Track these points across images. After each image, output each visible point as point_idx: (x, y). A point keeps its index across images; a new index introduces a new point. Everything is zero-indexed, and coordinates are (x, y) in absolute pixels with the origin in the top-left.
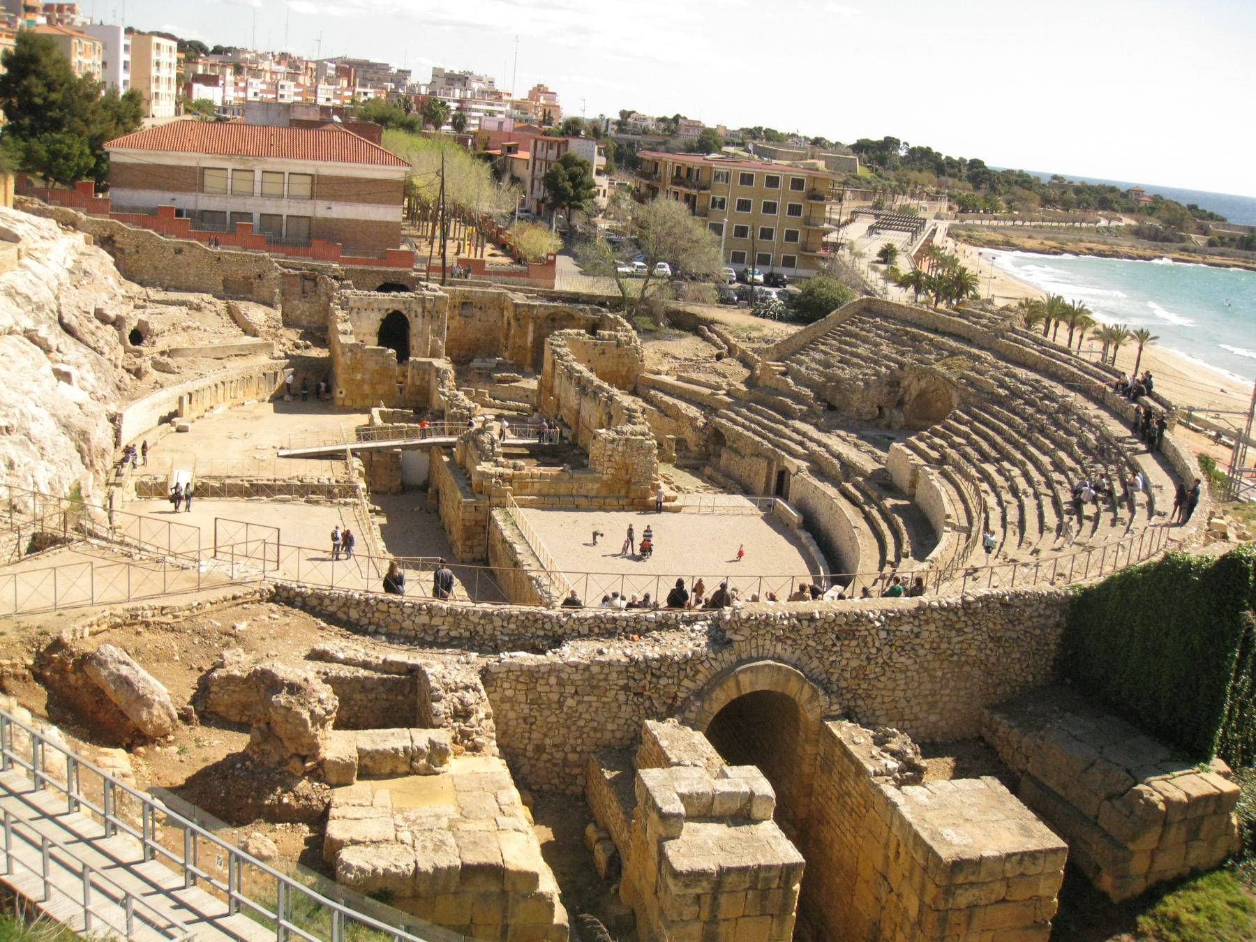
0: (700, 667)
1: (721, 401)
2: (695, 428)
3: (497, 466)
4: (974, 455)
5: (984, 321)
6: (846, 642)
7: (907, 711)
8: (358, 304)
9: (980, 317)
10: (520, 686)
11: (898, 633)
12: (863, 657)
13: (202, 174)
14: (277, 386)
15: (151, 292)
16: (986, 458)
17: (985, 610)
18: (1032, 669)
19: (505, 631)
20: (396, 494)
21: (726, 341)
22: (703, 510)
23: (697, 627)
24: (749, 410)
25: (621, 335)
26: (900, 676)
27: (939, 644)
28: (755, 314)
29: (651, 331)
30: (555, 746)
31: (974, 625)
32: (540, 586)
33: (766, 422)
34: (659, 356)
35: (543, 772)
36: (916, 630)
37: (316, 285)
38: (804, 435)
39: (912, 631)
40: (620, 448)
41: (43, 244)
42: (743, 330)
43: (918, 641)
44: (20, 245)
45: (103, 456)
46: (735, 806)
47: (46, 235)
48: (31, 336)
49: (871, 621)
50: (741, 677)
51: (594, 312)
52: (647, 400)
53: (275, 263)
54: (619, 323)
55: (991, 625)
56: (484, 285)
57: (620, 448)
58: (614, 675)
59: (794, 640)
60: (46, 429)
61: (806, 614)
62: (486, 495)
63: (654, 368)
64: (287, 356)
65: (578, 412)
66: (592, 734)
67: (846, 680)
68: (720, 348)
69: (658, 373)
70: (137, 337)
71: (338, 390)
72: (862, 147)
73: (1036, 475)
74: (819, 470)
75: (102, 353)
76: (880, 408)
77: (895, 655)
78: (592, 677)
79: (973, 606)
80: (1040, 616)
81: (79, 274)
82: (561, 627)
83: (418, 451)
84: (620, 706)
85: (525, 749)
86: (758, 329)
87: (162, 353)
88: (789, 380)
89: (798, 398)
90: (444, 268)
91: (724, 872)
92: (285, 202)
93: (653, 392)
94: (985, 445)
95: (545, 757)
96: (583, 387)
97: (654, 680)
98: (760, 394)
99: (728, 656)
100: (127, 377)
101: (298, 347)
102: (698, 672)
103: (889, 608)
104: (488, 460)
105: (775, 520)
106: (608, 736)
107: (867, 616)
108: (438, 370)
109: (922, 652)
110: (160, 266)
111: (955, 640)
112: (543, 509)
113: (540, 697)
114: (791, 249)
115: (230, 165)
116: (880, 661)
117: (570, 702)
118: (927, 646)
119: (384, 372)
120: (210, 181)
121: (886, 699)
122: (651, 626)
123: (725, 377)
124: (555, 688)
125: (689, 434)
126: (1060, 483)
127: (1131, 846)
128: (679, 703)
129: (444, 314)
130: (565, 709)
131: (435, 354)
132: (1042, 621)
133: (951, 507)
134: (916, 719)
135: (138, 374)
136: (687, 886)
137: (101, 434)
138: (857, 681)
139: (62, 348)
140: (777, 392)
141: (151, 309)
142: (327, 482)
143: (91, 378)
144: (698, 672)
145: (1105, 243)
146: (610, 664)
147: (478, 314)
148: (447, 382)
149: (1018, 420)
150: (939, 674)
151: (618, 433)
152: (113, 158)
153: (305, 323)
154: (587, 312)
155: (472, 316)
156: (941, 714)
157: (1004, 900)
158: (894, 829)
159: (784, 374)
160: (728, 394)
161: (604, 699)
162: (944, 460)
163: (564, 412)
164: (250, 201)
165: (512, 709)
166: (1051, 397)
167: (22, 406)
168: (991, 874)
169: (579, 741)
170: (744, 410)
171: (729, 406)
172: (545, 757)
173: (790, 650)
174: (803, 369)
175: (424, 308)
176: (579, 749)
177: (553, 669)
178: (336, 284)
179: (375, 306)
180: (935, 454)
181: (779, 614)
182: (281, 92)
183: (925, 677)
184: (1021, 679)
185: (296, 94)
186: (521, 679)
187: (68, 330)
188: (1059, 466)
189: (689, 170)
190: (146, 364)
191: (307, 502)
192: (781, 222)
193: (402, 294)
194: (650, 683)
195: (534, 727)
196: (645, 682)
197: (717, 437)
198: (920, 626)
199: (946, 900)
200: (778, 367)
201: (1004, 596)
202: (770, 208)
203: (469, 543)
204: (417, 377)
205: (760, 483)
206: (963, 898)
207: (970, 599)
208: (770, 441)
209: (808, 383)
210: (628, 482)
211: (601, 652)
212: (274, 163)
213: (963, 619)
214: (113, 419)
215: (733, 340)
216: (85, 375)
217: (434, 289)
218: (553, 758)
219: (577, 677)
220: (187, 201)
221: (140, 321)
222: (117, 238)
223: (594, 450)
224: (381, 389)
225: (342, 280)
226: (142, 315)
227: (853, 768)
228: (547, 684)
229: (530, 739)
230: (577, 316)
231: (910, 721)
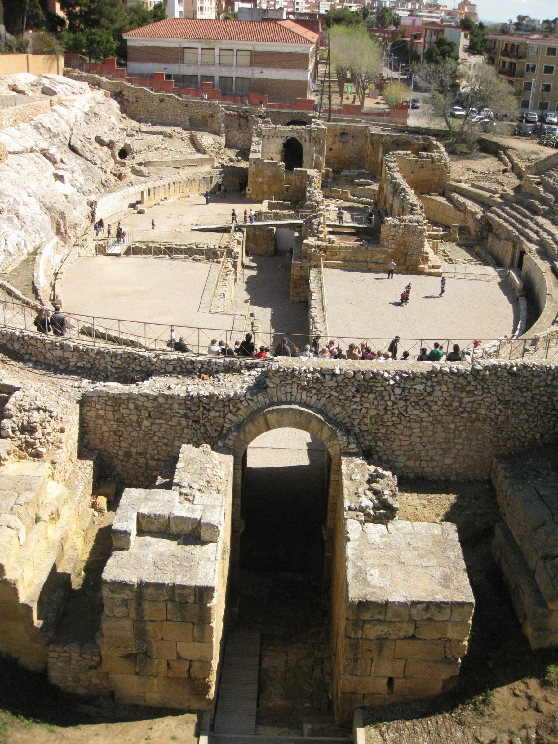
0: (239, 405)
1: (495, 202)
2: (475, 220)
3: (318, 240)
6: (366, 395)
7: (423, 453)
8: (268, 134)
10: (108, 408)
12: (381, 408)
13: (183, 53)
14: (213, 185)
15: (144, 127)
17: (493, 377)
18: (540, 430)
19: (114, 365)
20: (271, 256)
21: (512, 161)
22: (459, 275)
23: (253, 373)
24: (512, 208)
25: (435, 155)
26: (414, 425)
28: (540, 144)
29: (465, 153)
30: (140, 454)
31: (483, 389)
32: (314, 323)
33: (519, 216)
34: (464, 170)
35: (132, 472)
36: (429, 389)
37: (248, 121)
38: (541, 227)
39: (425, 390)
40: (400, 231)
41: (72, 97)
42: (526, 154)
43: (431, 398)
44: (52, 98)
45: (75, 228)
46: (188, 528)
47: (76, 91)
48: (45, 153)
49: (386, 380)
50: (269, 416)
51: (424, 140)
52: (450, 200)
53: (222, 107)
54: (437, 147)
55: (500, 390)
56: (356, 122)
57: (400, 231)
58: (176, 406)
59: (318, 390)
60: (32, 210)
61: (328, 370)
62: (310, 259)
63: (458, 178)
64: (223, 166)
65: (392, 206)
66: (164, 447)
67: (365, 424)
68: (507, 165)
69: (460, 181)
70: (123, 154)
71: (247, 188)
74: (545, 253)
75: (95, 164)
77: (410, 409)
78: (162, 405)
80: (547, 385)
81: (92, 115)
82: (153, 365)
83: (288, 229)
84: (183, 429)
85: (117, 454)
86: (537, 153)
87: (140, 164)
88: (541, 188)
89: (544, 201)
90: (330, 111)
91: (143, 586)
92: (234, 69)
93: (453, 194)
95: (132, 461)
96: (397, 189)
97: (205, 412)
98: (522, 199)
99: (261, 398)
100: (113, 178)
101: (232, 160)
102: (238, 409)
103: (404, 369)
104: (314, 236)
105: (506, 286)
107: (383, 375)
108: (309, 176)
109: (435, 408)
110: (151, 110)
111: (466, 400)
112: (345, 270)
113: (124, 417)
115: (199, 46)
116: (396, 412)
117: (146, 423)
118: (440, 403)
119: (276, 177)
120: (189, 56)
121: (403, 443)
122: (219, 369)
123: (503, 185)
124: (134, 412)
125: (471, 223)
127: (550, 606)
128: (225, 432)
129: (323, 140)
130: (143, 428)
131: (317, 166)
132: (550, 390)
134: (432, 460)
135: (120, 177)
138: (376, 427)
139: (65, 160)
140: (532, 196)
141: (138, 136)
142: (212, 247)
143: (81, 179)
144: (238, 409)
146: (172, 397)
147: (351, 141)
148: (313, 184)
150: (452, 426)
151: (400, 220)
153: (240, 146)
154: (419, 139)
155: (347, 142)
156: (455, 458)
157: (413, 637)
159: (539, 184)
160: (502, 197)
161: (170, 423)
163: (388, 206)
164: (212, 68)
165: (105, 424)
167: (17, 197)
168: (398, 615)
169: (156, 452)
170: (507, 209)
171: (499, 205)
172: (132, 461)
173: (315, 397)
174: (551, 181)
175: (310, 136)
176: (156, 457)
177: (130, 397)
178: (260, 120)
179: (279, 134)
181: (303, 368)
182: (296, 7)
183: (439, 428)
184: (529, 436)
185: (306, 8)
186: (108, 403)
187: (73, 149)
189: (513, 45)
190: (127, 171)
191: (193, 259)
193: (299, 127)
194: (203, 414)
195: (122, 439)
196: (199, 413)
197: (487, 226)
198: (432, 386)
199: (356, 632)
200: (534, 178)
201: (512, 367)
203: (296, 290)
204: (297, 181)
205: (507, 260)
206: (373, 632)
207: (478, 367)
208: (518, 230)
210: (406, 255)
211: (169, 388)
212: (227, 44)
213: (473, 383)
214: (92, 205)
215: (516, 160)
216: (77, 177)
217: (320, 124)
218: (138, 462)
219: (149, 404)
220: (174, 69)
221: (125, 144)
222: (125, 93)
223: (384, 231)
224: (275, 188)
225: (265, 118)
226: (128, 141)
228: (128, 408)
229: (120, 447)
230: (412, 142)
231: (427, 461)
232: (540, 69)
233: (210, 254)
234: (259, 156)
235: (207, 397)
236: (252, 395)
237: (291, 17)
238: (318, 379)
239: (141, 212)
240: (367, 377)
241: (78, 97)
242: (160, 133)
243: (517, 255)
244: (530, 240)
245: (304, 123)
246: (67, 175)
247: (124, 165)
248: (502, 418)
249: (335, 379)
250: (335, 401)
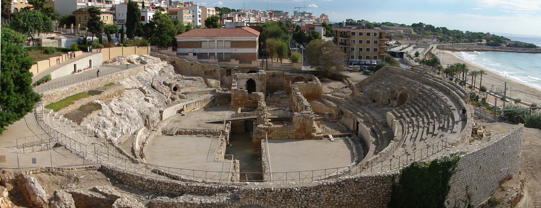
4: (410, 115)
5: (419, 71)
9: (418, 70)
11: (310, 196)
15: (184, 77)
16: (413, 115)
17: (348, 185)
21: (348, 82)
27: (329, 200)
36: (318, 194)
39: (316, 194)
41: (154, 65)
48: (141, 89)
55: (351, 190)
61: (268, 189)
69: (327, 93)
70: (175, 89)
73: (426, 121)
76: (389, 101)
77: (310, 204)
79: (342, 183)
94: (414, 111)
100: (171, 100)
109: (322, 203)
114: (376, 54)
115: (208, 40)
118: (324, 200)
126: (431, 123)
133: (397, 133)
135: (173, 99)
137: (155, 116)
139: (150, 92)
143: (156, 101)
149: (424, 102)
152: (178, 40)
162: (401, 117)
166: (434, 94)
173: (263, 202)
180: (399, 115)
187: (153, 87)
188: (433, 117)
189: (344, 32)
192: (372, 46)
198: (320, 193)
212: (220, 38)
215: (351, 82)
220: (197, 51)
222: (176, 62)
226: (177, 83)
232: (357, 42)
233: (215, 134)
234: (236, 88)
235: (210, 204)
236: (232, 202)
237: (248, 25)
238: (263, 194)
239: (183, 115)
240: (288, 191)
241: (156, 65)
243: (356, 124)
244: (360, 117)
245: (255, 72)
246: (150, 99)
247: (175, 94)
248: (354, 203)
249: (271, 193)
250: (273, 204)
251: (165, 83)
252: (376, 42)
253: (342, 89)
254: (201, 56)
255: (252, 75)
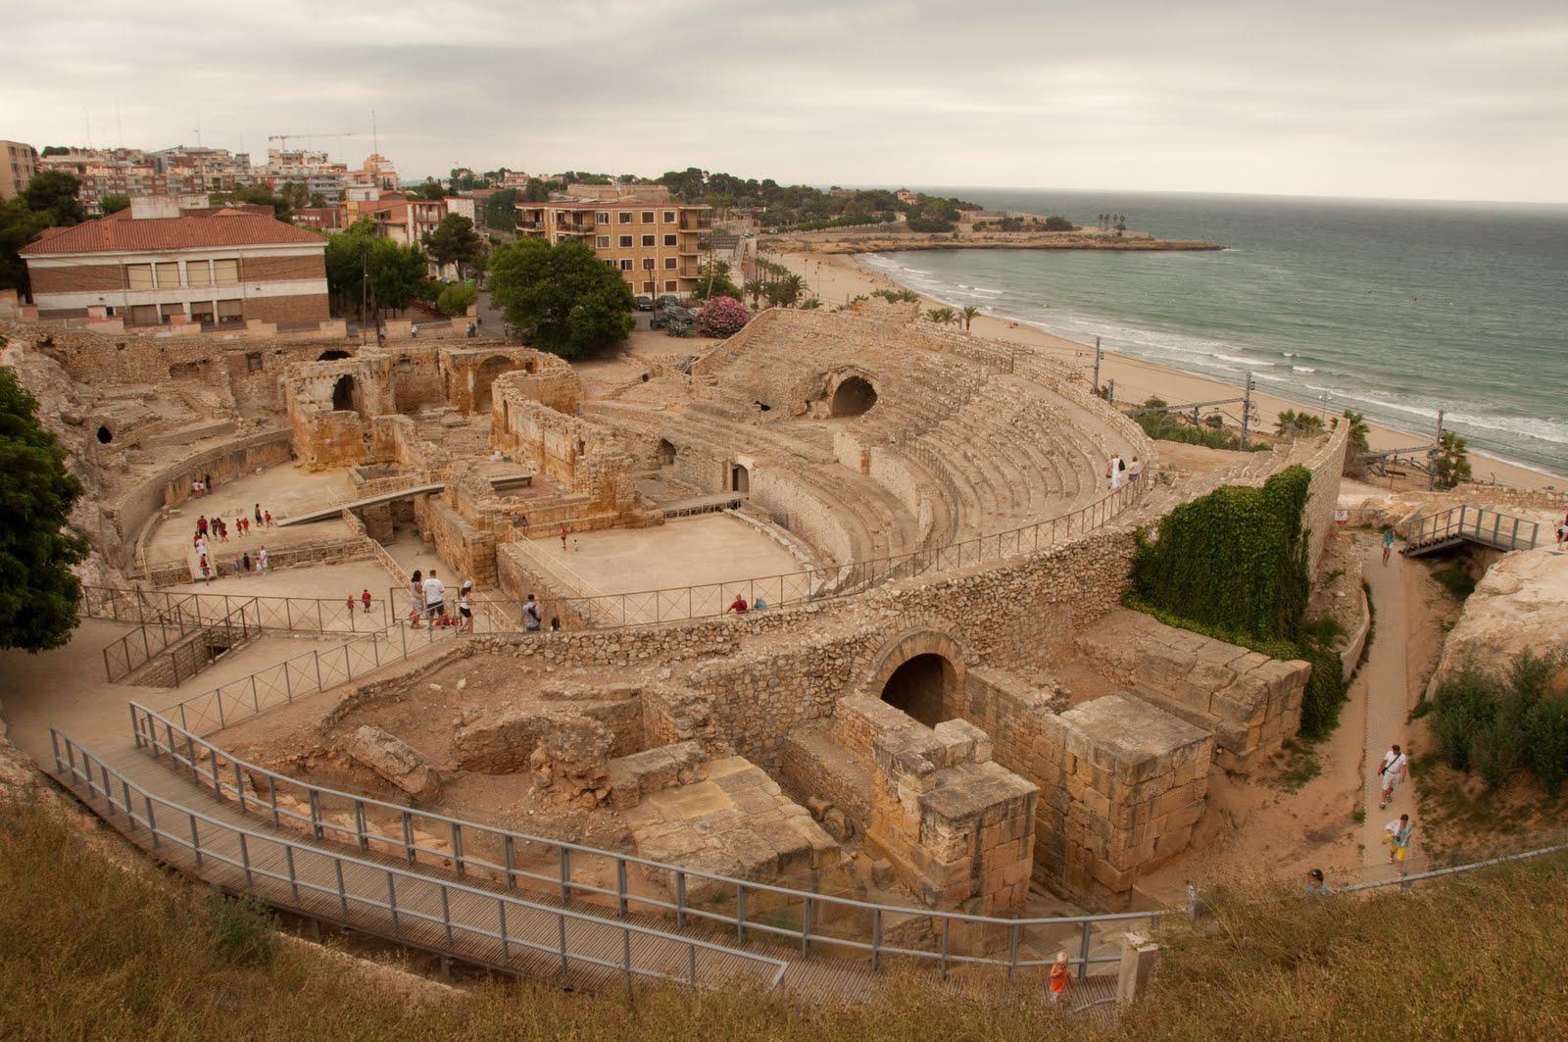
10: (720, 690)
70: (105, 435)
72: (671, 179)
76: (807, 402)
77: (1011, 606)
87: (133, 446)
106: (798, 718)
124: (750, 686)
134: (1030, 655)
136: (958, 829)
145: (889, 239)
152: (31, 264)
158: (1069, 749)
191: (328, 564)
202: (649, 241)
209: (738, 387)
220: (116, 299)
222: (57, 342)
227: (1011, 706)
242: (138, 396)
243: (730, 475)
245: (344, 355)
251: (67, 420)
252: (670, 240)
253: (635, 383)
254: (132, 316)
255: (340, 367)
